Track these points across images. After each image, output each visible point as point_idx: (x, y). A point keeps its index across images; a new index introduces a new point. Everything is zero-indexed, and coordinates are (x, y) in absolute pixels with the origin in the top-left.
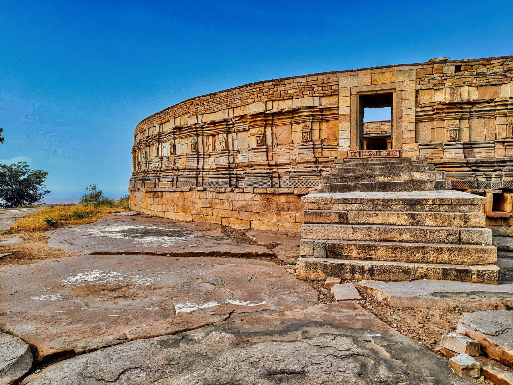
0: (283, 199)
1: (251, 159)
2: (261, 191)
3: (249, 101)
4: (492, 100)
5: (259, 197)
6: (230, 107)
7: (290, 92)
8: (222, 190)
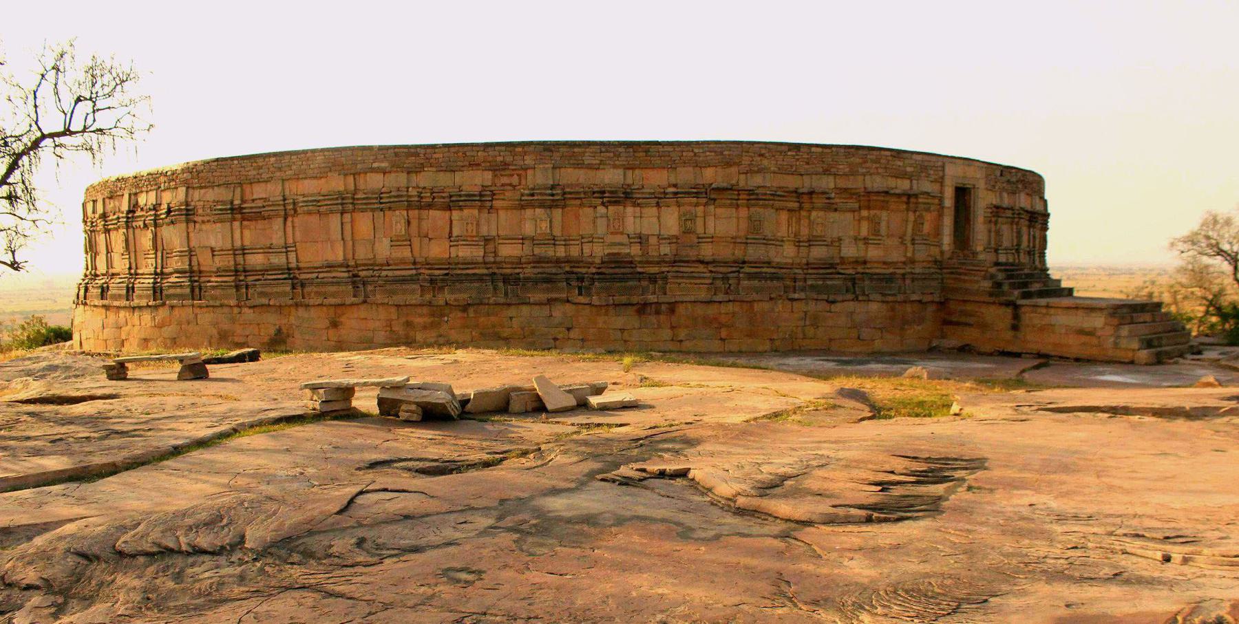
0: (908, 308)
1: (862, 254)
2: (890, 299)
3: (861, 170)
4: (1012, 209)
5: (884, 306)
6: (826, 172)
7: (909, 169)
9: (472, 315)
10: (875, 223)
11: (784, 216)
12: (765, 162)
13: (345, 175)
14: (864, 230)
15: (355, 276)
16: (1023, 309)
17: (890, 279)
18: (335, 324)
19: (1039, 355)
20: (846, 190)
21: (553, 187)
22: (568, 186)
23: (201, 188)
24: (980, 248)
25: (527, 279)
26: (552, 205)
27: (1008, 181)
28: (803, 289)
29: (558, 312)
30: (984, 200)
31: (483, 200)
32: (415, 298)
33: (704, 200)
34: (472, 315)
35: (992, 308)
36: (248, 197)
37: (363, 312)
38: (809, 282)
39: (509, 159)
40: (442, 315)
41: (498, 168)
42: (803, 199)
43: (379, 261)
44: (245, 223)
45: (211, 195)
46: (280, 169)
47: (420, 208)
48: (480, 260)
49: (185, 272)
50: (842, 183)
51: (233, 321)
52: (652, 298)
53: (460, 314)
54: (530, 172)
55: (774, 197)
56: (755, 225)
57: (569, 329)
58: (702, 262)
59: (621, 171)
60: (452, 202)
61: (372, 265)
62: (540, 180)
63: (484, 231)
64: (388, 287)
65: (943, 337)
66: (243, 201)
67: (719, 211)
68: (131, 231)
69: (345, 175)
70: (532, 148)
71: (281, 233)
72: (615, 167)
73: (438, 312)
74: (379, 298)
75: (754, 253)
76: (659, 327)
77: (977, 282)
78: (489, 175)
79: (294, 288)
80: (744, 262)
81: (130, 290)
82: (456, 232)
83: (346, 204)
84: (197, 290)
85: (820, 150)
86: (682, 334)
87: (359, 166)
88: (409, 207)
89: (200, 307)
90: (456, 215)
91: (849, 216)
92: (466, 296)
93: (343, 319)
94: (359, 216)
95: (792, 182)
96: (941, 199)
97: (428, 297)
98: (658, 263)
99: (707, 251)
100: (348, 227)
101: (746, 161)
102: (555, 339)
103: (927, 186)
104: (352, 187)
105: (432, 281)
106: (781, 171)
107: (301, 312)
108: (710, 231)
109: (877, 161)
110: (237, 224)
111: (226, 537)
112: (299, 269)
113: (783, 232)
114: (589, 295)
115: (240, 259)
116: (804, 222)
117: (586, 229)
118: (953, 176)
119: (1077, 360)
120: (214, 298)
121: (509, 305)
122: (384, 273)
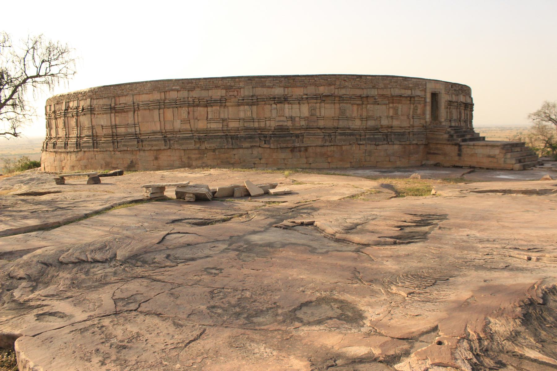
0: (411, 147)
1: (390, 123)
2: (403, 143)
3: (389, 86)
4: (457, 102)
6: (374, 87)
7: (410, 85)
9: (217, 153)
10: (396, 110)
11: (355, 107)
12: (347, 84)
13: (160, 92)
14: (391, 113)
15: (165, 137)
16: (463, 147)
17: (403, 134)
18: (156, 158)
19: (471, 167)
20: (382, 95)
21: (252, 96)
22: (259, 95)
23: (97, 99)
24: (443, 120)
25: (242, 137)
26: (252, 104)
27: (455, 90)
28: (364, 140)
29: (256, 151)
30: (444, 98)
31: (222, 102)
32: (192, 146)
33: (320, 101)
34: (217, 153)
35: (449, 146)
36: (118, 103)
37: (169, 153)
38: (367, 137)
39: (233, 84)
40: (204, 154)
41: (228, 88)
42: (364, 99)
43: (176, 130)
44: (116, 114)
45: (101, 102)
46: (132, 90)
47: (194, 106)
48: (221, 129)
49: (90, 136)
50: (381, 92)
51: (111, 157)
52: (297, 145)
53: (212, 153)
54: (242, 90)
55: (350, 99)
56: (342, 112)
57: (260, 159)
58: (319, 128)
59: (282, 89)
60: (208, 104)
61: (173, 132)
62: (247, 93)
63: (222, 116)
64: (180, 142)
65: (427, 160)
66: (116, 104)
67: (327, 105)
68: (66, 118)
69: (160, 92)
70: (243, 79)
71: (133, 118)
72: (280, 87)
73: (202, 152)
74: (176, 146)
75: (342, 124)
76: (301, 157)
77: (442, 135)
78: (224, 91)
79: (138, 142)
80: (338, 128)
81: (66, 144)
82: (209, 117)
83: (161, 105)
84: (95, 144)
85: (371, 78)
86: (311, 160)
87: (167, 88)
88: (189, 106)
89: (97, 152)
90: (209, 109)
91: (384, 107)
92: (214, 145)
93: (160, 156)
94: (166, 110)
95: (358, 92)
96: (425, 98)
97: (198, 145)
98: (300, 129)
99: (321, 124)
100: (162, 115)
101: (338, 83)
102: (255, 164)
103: (418, 93)
104: (163, 97)
105: (199, 139)
106: (354, 87)
107: (142, 153)
108: (323, 114)
109: (396, 82)
110: (113, 115)
111: (108, 255)
112: (140, 134)
113: (355, 114)
114: (269, 144)
115: (114, 130)
116: (364, 110)
117: (268, 114)
118: (430, 88)
119: (487, 169)
120: (103, 147)
121: (234, 149)
122: (178, 135)
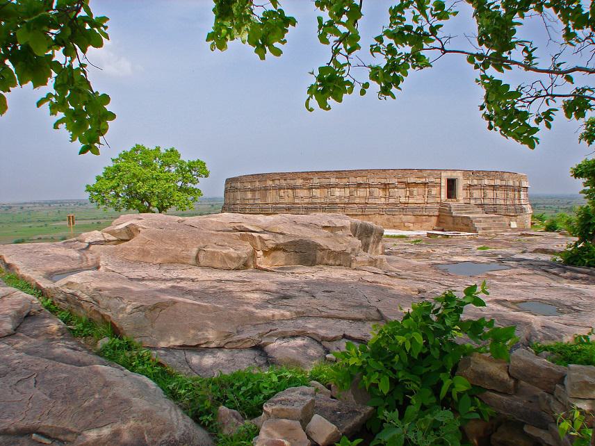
0: (424, 217)
8: (397, 213)
10: (411, 193)
50: (400, 180)
75: (370, 201)
99: (357, 201)
103: (433, 180)
116: (387, 192)
